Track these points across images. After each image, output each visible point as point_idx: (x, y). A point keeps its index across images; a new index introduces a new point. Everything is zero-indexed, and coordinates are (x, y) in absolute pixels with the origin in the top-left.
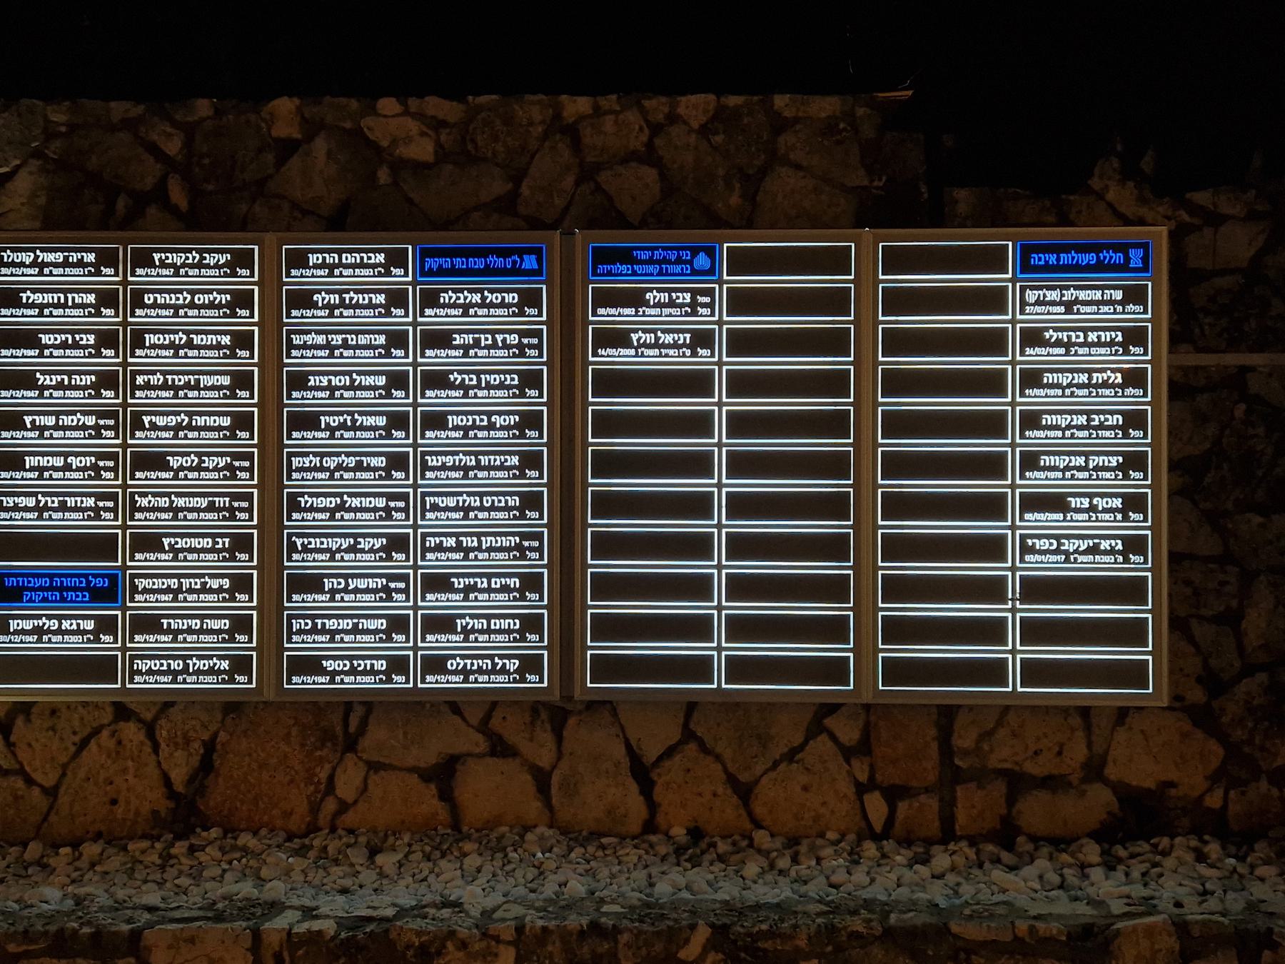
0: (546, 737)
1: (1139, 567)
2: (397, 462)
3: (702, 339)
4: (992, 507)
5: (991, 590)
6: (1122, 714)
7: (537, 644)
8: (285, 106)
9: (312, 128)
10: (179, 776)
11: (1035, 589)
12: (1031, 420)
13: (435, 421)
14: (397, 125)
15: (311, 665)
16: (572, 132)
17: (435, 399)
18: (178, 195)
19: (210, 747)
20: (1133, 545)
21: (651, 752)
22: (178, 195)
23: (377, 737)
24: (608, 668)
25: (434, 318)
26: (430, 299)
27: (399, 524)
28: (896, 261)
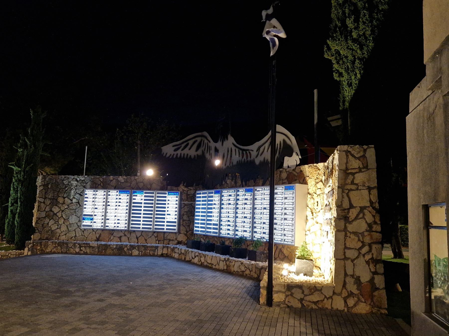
0: (129, 234)
2: (116, 209)
7: (126, 225)
9: (114, 179)
10: (97, 237)
13: (119, 206)
15: (108, 226)
16: (136, 180)
21: (138, 236)
23: (115, 234)
24: (132, 228)
26: (120, 195)
27: (116, 215)
28: (158, 193)
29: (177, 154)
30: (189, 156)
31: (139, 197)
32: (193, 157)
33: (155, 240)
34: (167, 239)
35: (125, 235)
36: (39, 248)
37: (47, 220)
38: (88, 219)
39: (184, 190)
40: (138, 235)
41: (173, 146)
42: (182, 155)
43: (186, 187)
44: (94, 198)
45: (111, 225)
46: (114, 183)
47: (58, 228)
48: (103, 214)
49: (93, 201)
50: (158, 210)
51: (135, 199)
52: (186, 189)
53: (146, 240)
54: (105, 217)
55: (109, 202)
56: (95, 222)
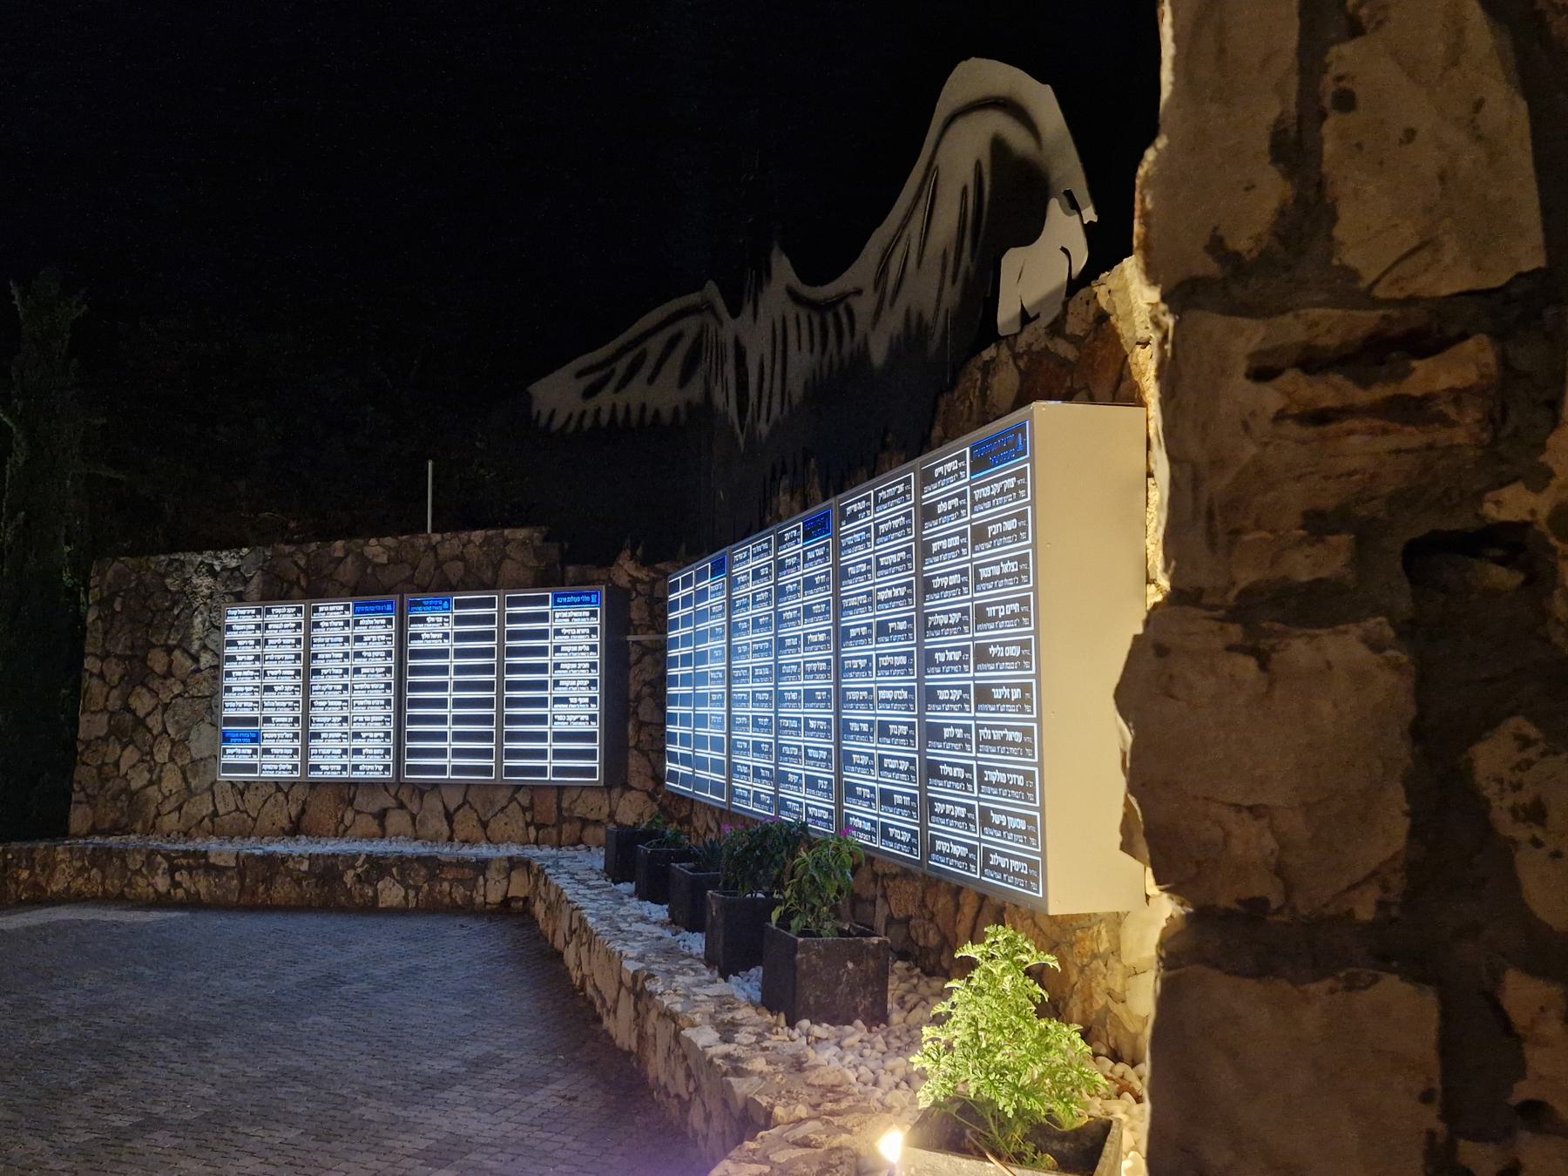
0: (417, 801)
1: (594, 727)
3: (446, 636)
4: (542, 702)
5: (542, 737)
6: (584, 787)
7: (389, 760)
8: (339, 543)
10: (293, 814)
11: (559, 737)
12: (557, 666)
14: (376, 549)
16: (434, 548)
17: (358, 662)
18: (303, 583)
19: (305, 802)
20: (592, 718)
21: (452, 808)
22: (303, 583)
23: (360, 801)
25: (358, 631)
28: (513, 602)
29: (598, 411)
30: (649, 413)
31: (435, 629)
32: (666, 416)
33: (522, 824)
34: (571, 820)
35: (402, 806)
36: (25, 874)
37: (114, 750)
38: (241, 738)
39: (634, 581)
40: (454, 800)
41: (579, 375)
42: (620, 415)
43: (645, 562)
44: (257, 642)
45: (330, 762)
46: (348, 571)
47: (151, 783)
48: (298, 712)
49: (257, 658)
50: (514, 679)
51: (417, 637)
52: (642, 574)
53: (485, 825)
54: (306, 728)
55: (315, 656)
56: (267, 751)
